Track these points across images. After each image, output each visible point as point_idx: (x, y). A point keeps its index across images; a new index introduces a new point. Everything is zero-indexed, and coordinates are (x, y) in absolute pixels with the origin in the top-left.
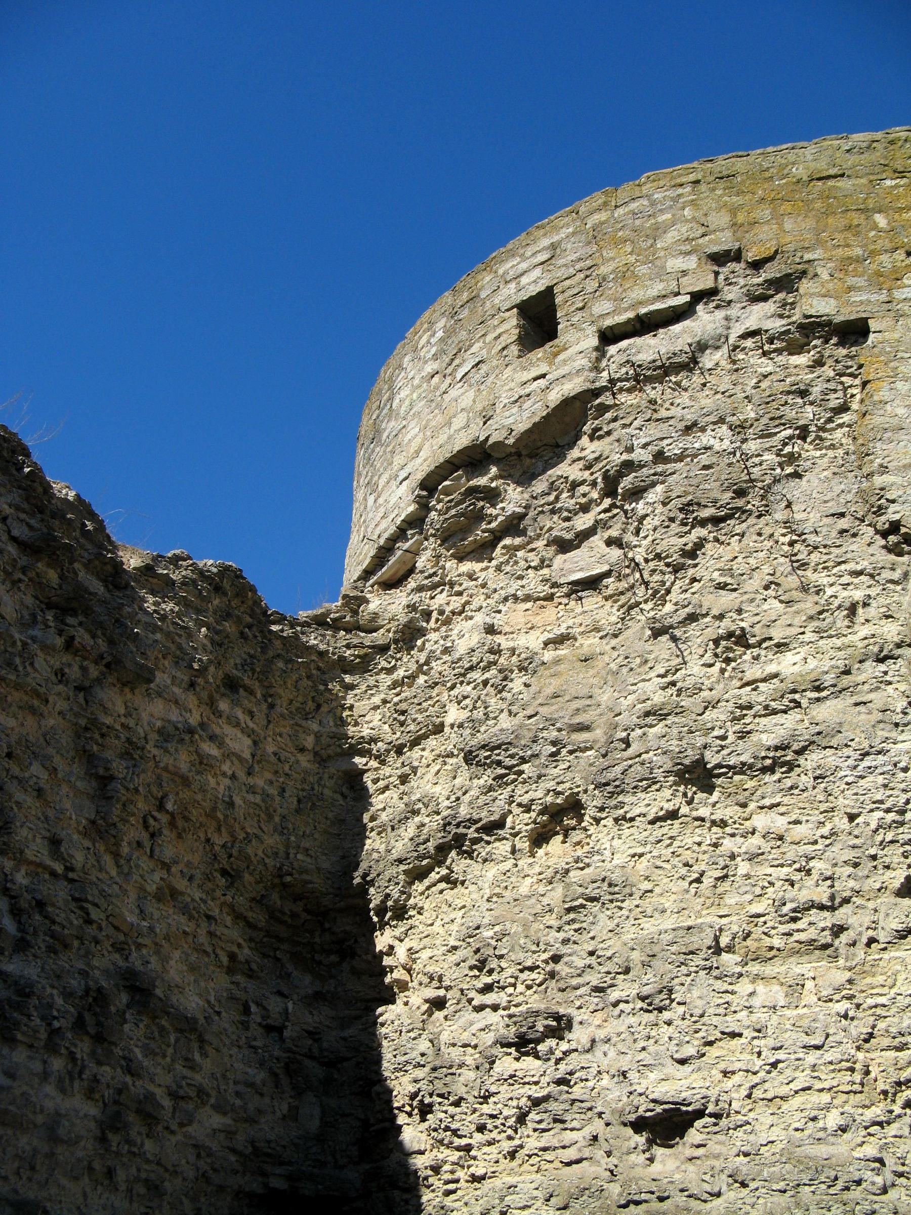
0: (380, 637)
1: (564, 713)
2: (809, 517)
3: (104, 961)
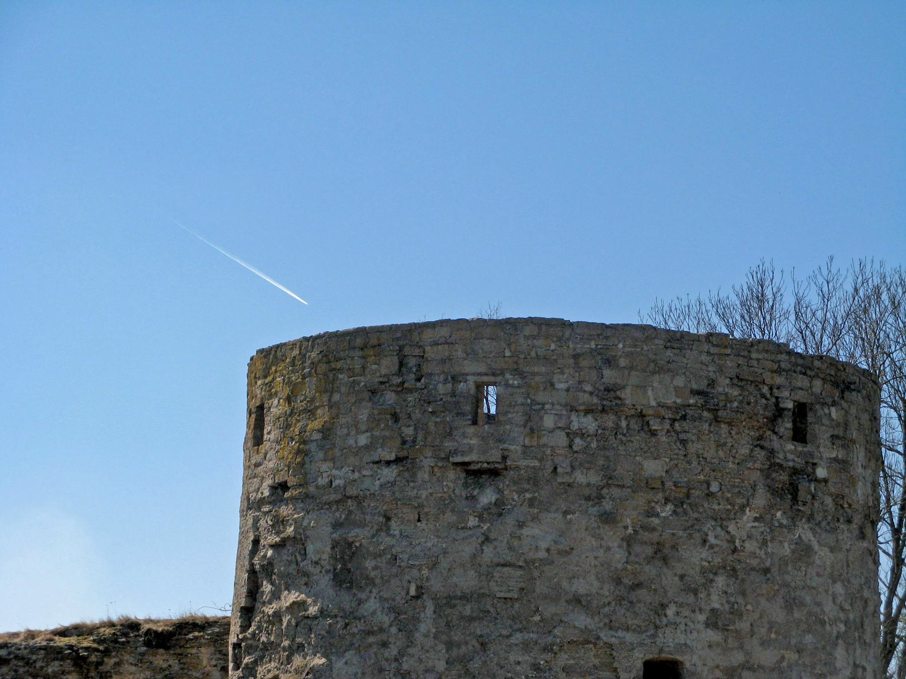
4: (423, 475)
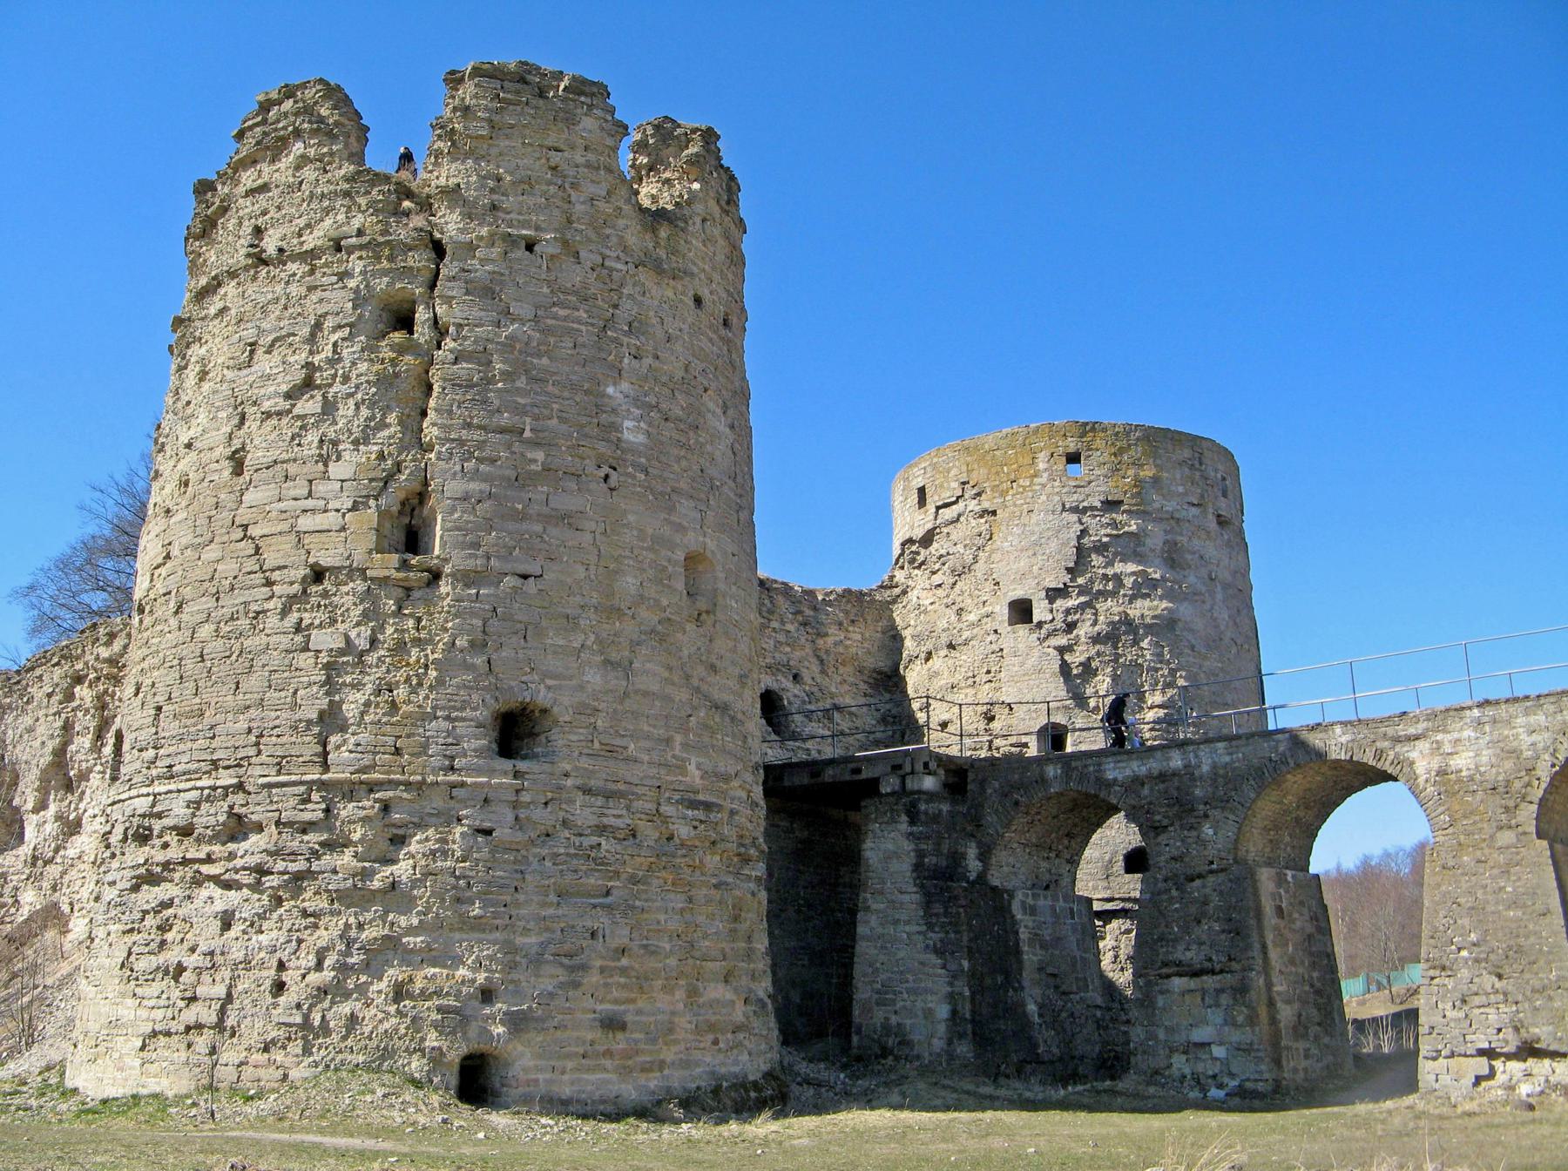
0: (897, 591)
1: (929, 627)
2: (979, 575)
3: (829, 701)
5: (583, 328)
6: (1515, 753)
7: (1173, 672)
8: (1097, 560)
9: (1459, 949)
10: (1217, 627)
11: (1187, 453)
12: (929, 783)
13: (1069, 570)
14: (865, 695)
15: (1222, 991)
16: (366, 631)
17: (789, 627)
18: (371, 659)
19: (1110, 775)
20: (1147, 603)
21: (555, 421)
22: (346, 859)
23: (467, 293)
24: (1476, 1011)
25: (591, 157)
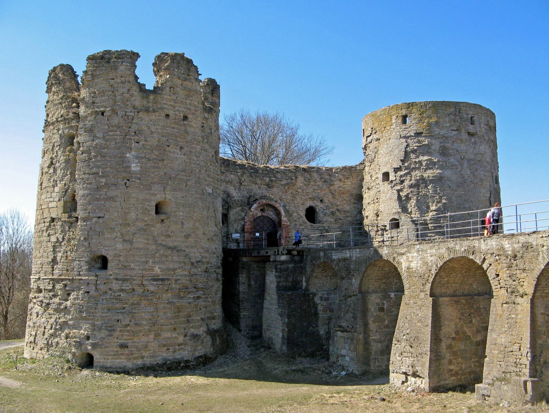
4: (463, 134)
5: (118, 137)
6: (426, 263)
7: (441, 198)
8: (412, 156)
9: (404, 335)
10: (464, 177)
11: (452, 110)
12: (283, 258)
13: (401, 160)
14: (354, 203)
15: (348, 338)
16: (61, 236)
17: (318, 183)
18: (63, 244)
19: (334, 257)
20: (431, 171)
21: (109, 169)
22: (57, 300)
23: (85, 132)
24: (404, 358)
25: (123, 79)
